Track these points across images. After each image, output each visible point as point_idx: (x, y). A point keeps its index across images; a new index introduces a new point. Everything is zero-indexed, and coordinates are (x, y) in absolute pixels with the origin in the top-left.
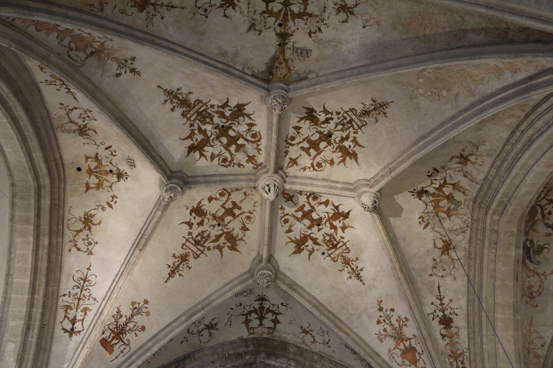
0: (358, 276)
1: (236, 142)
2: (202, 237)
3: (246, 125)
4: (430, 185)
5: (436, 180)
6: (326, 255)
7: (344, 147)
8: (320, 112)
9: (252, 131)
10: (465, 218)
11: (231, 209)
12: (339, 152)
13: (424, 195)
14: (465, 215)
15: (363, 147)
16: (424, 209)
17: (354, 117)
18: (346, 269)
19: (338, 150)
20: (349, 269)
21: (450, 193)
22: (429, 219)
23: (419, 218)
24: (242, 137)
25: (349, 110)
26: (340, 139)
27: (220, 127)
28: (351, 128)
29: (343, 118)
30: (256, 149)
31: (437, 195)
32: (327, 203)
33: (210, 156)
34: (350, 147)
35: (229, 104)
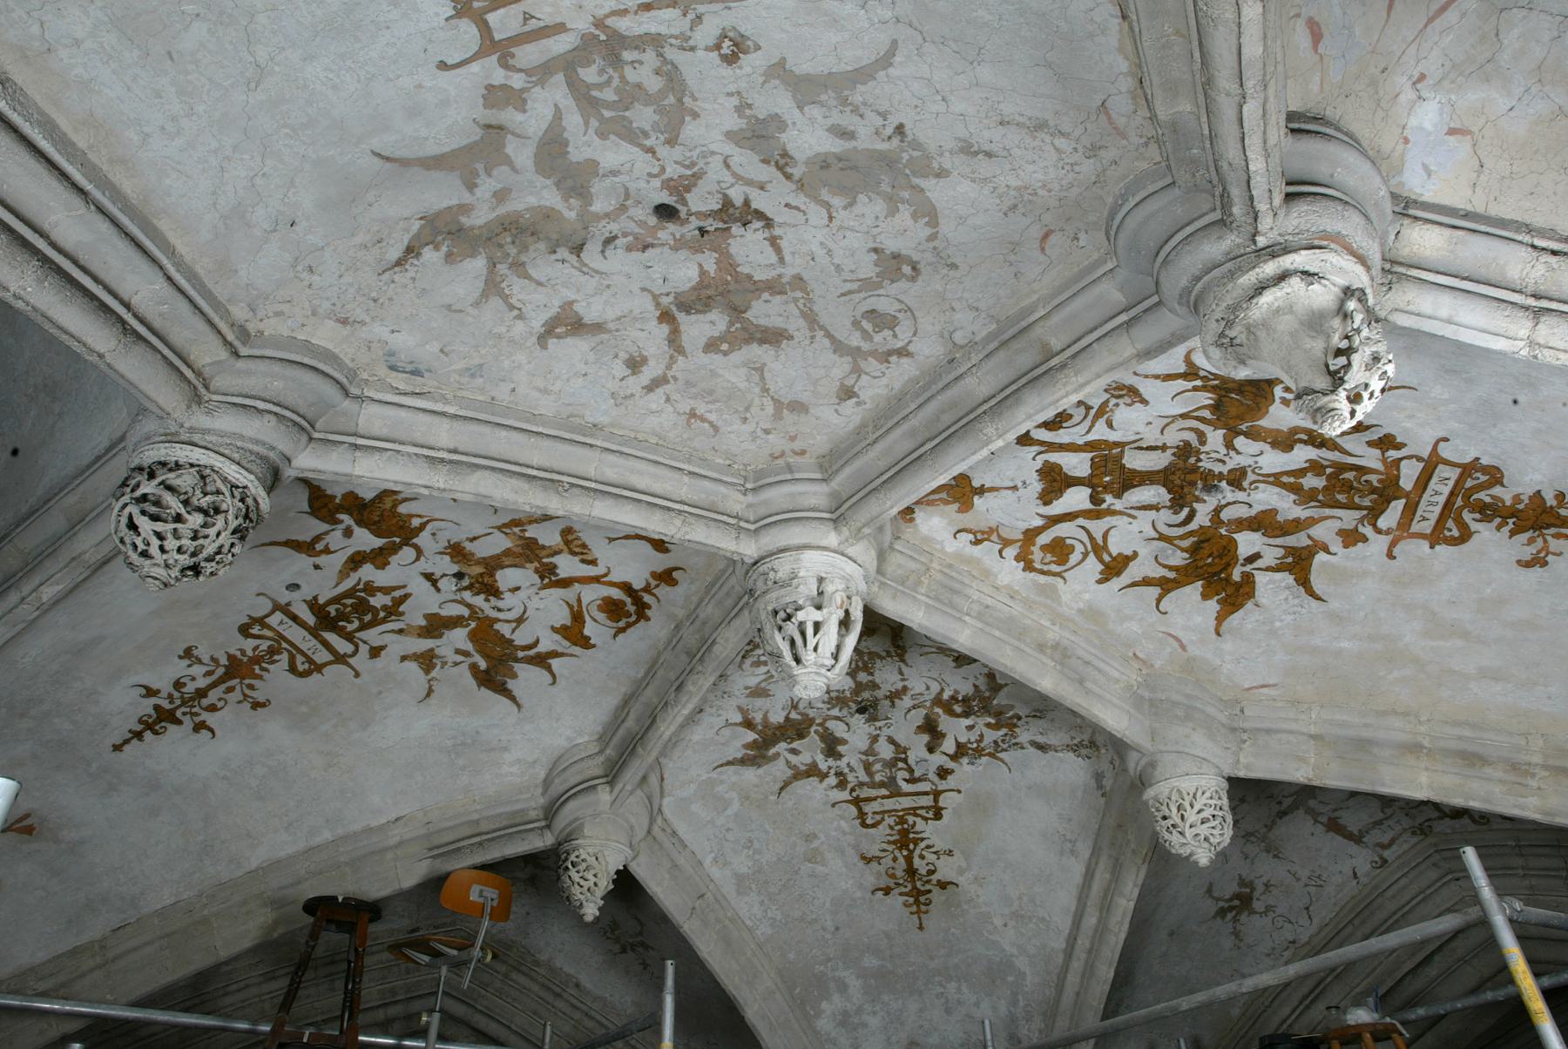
0: (161, 719)
1: (1092, 486)
2: (632, 95)
3: (1128, 552)
6: (285, 597)
7: (801, 736)
8: (982, 736)
9: (1085, 555)
11: (737, 311)
12: (787, 719)
15: (782, 789)
17: (906, 802)
18: (198, 670)
19: (794, 715)
20: (202, 683)
24: (1090, 511)
25: (941, 804)
26: (838, 735)
27: (1224, 484)
28: (864, 778)
29: (917, 774)
30: (991, 530)
32: (574, 633)
33: (1142, 390)
34: (794, 752)
35: (1287, 579)
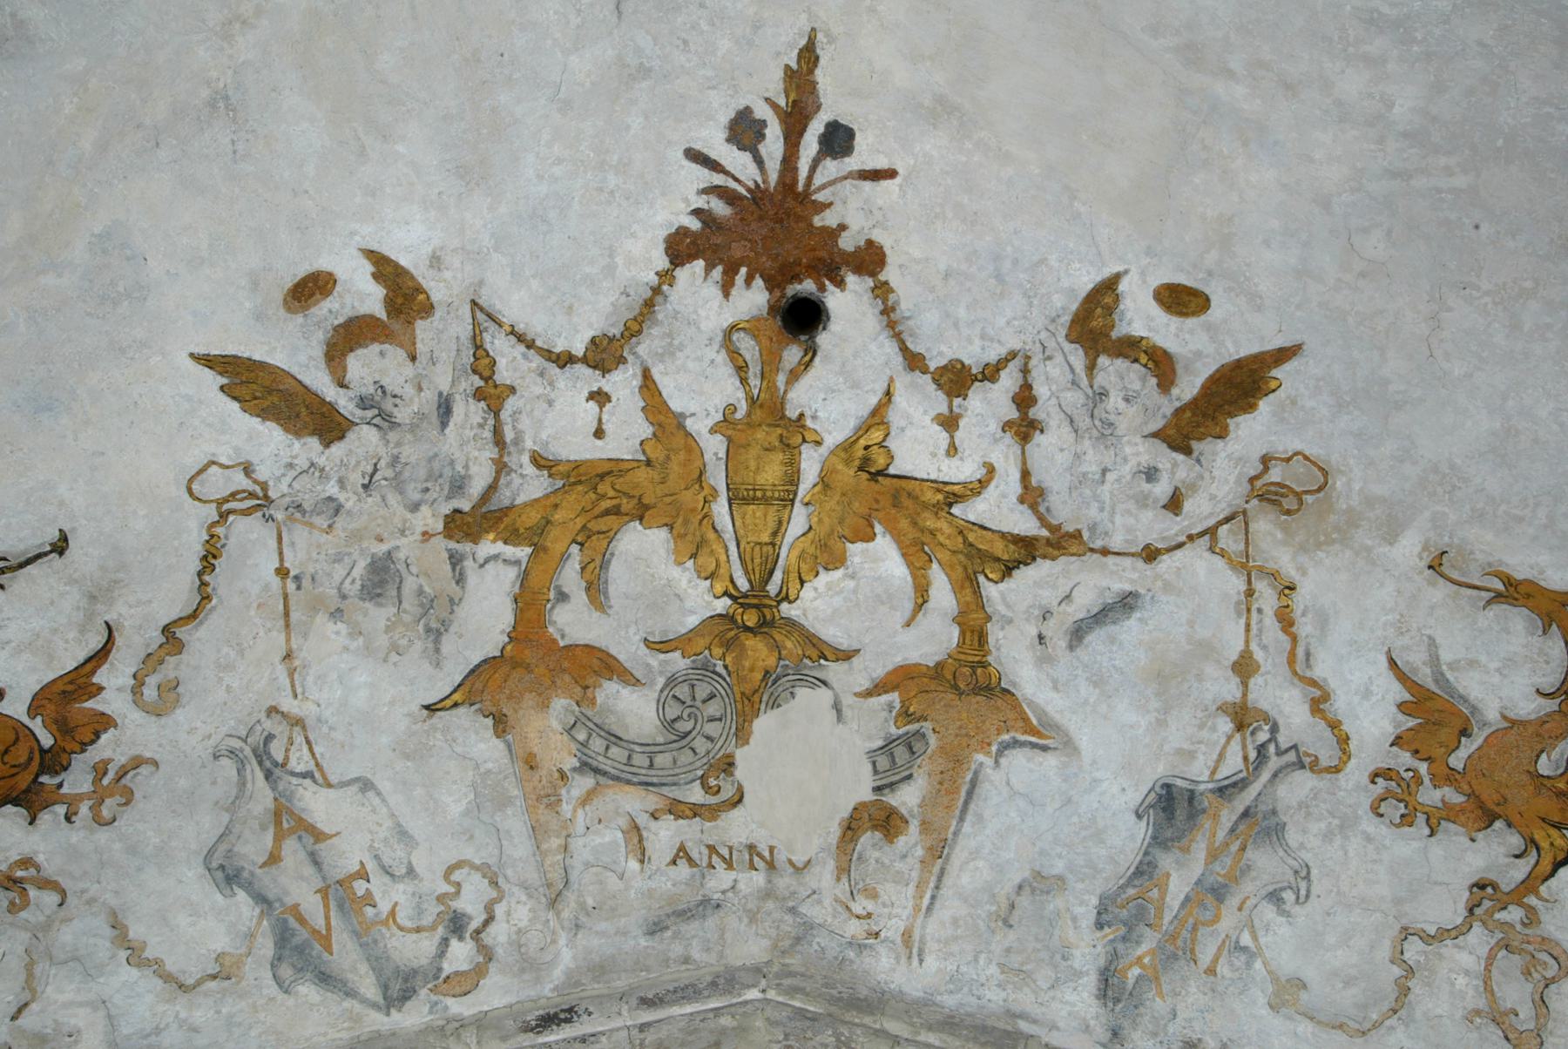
4: (914, 361)
5: (1024, 428)
10: (517, 913)
13: (753, 299)
14: (554, 902)
16: (537, 324)
21: (832, 634)
22: (385, 421)
23: (385, 269)
31: (771, 474)
